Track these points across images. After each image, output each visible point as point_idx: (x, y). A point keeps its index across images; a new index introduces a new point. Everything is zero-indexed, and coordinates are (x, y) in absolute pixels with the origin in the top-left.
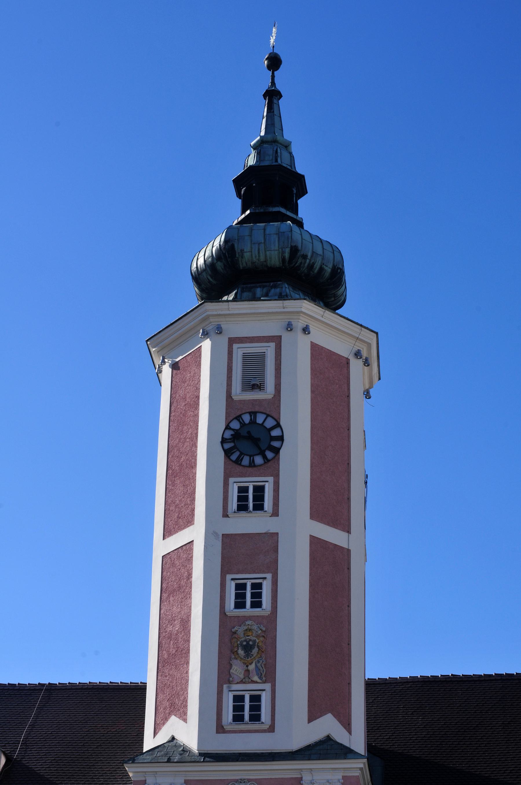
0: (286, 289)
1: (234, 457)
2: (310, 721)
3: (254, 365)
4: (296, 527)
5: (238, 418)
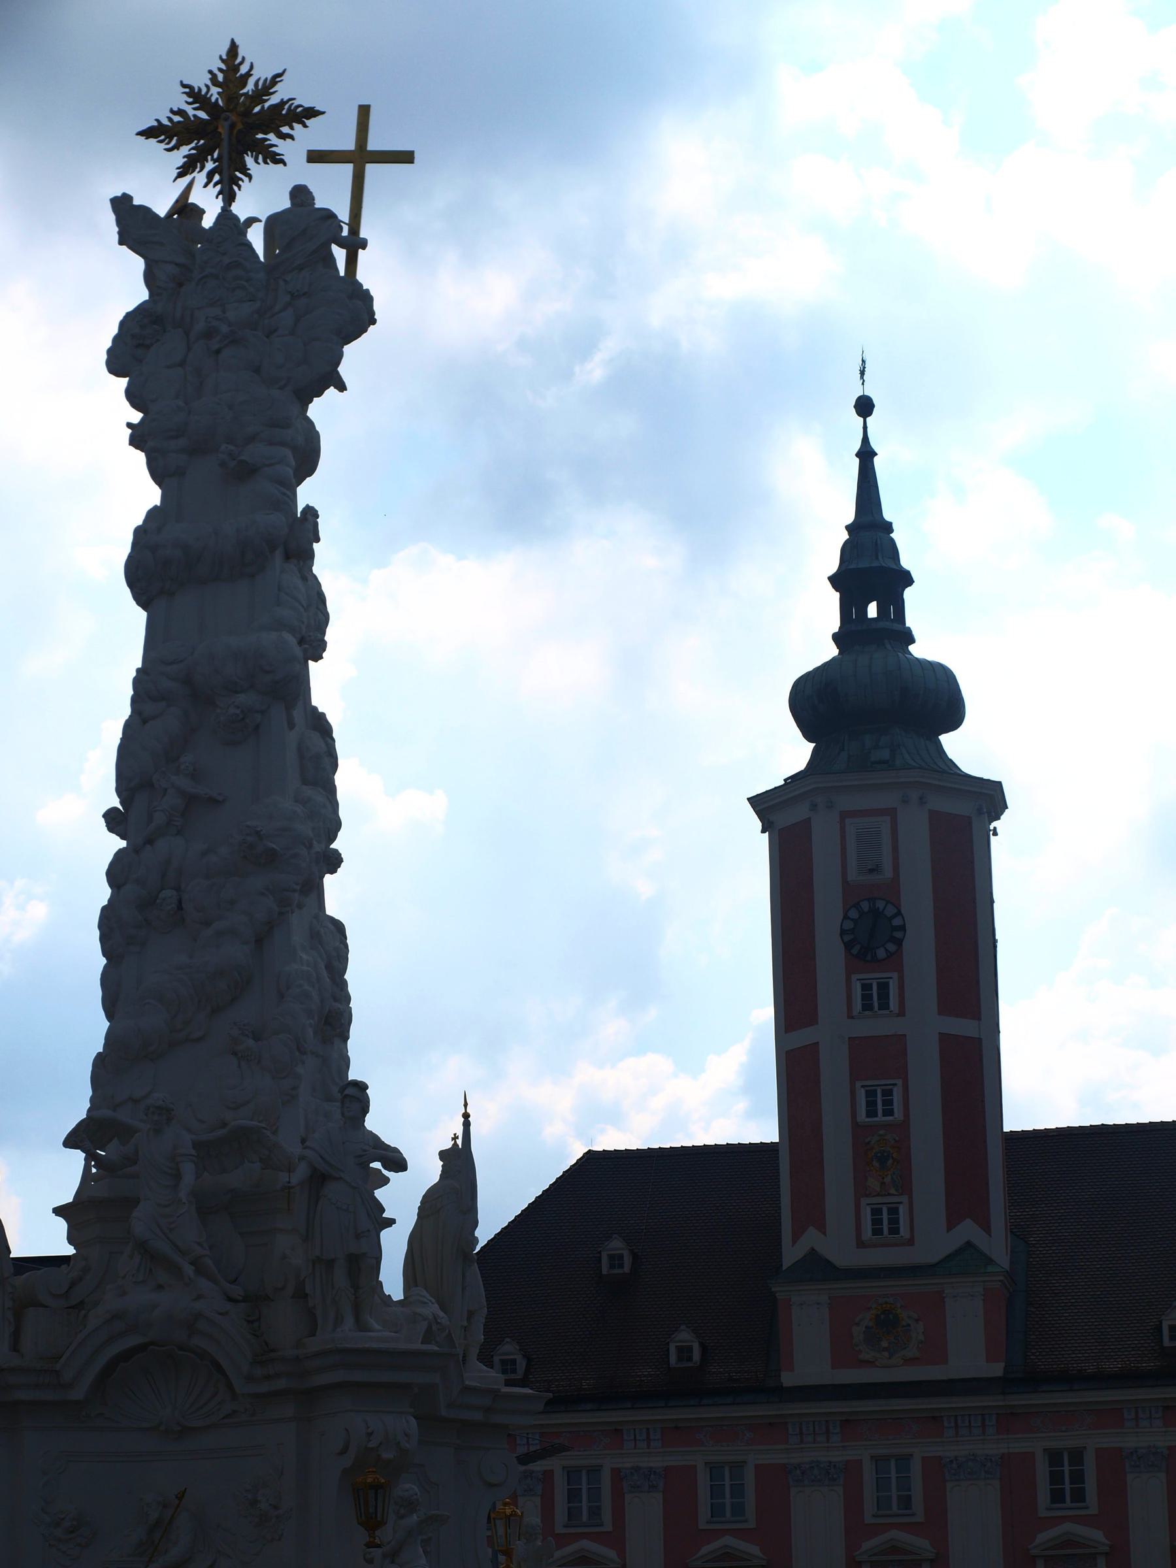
1: (855, 951)
2: (949, 1229)
4: (924, 1025)
5: (856, 905)
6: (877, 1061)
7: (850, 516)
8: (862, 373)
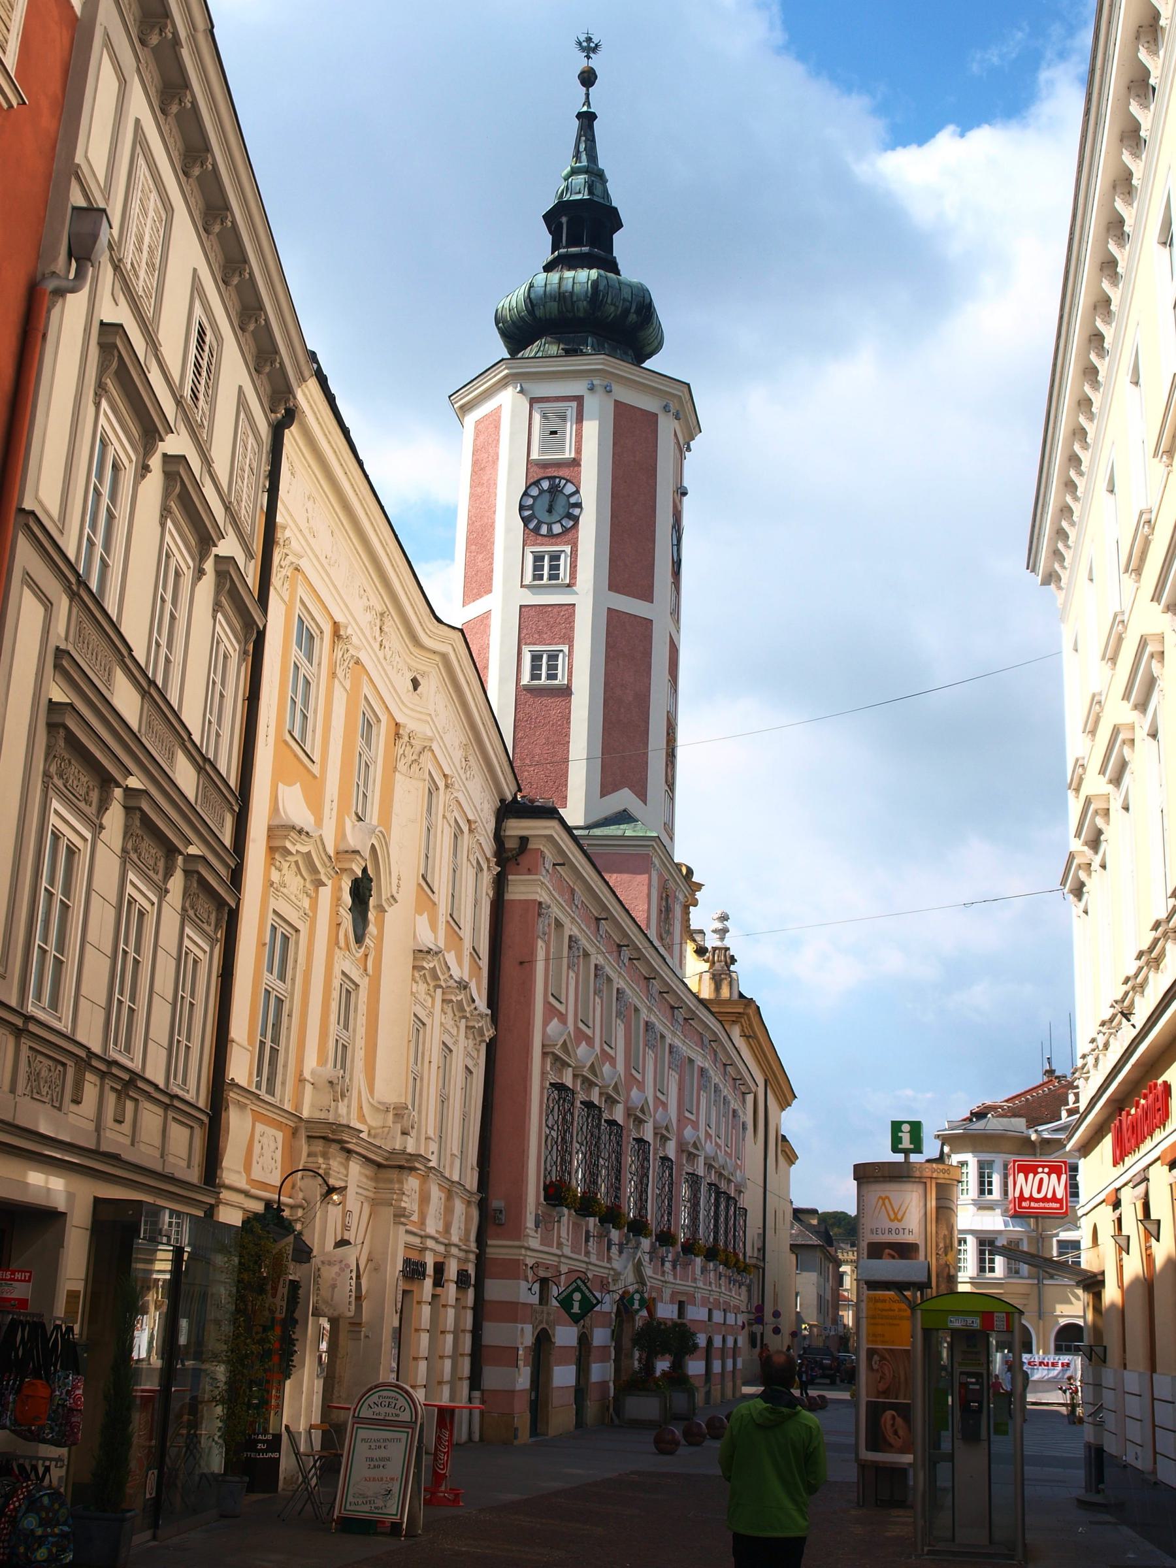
2: (603, 795)
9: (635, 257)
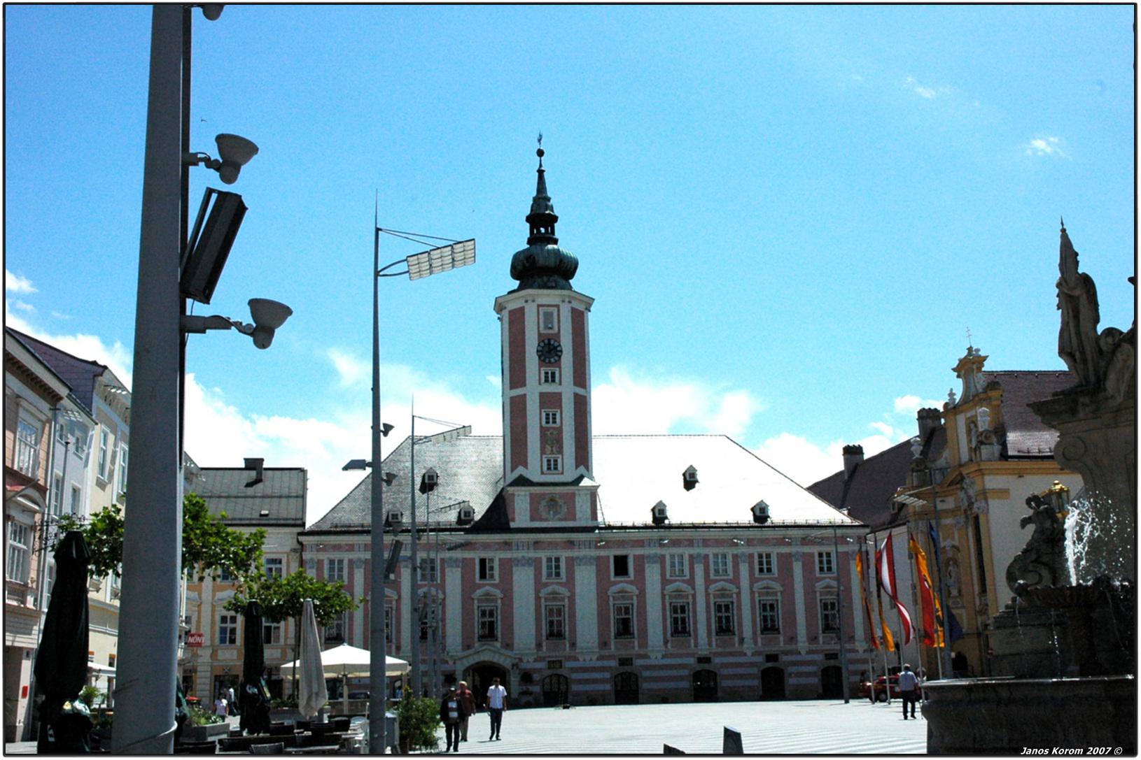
0: (556, 277)
3: (548, 316)
4: (567, 389)
6: (550, 401)
7: (534, 194)
8: (539, 140)
9: (567, 241)
